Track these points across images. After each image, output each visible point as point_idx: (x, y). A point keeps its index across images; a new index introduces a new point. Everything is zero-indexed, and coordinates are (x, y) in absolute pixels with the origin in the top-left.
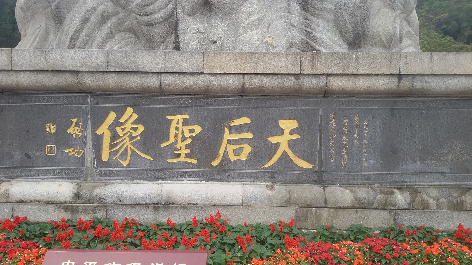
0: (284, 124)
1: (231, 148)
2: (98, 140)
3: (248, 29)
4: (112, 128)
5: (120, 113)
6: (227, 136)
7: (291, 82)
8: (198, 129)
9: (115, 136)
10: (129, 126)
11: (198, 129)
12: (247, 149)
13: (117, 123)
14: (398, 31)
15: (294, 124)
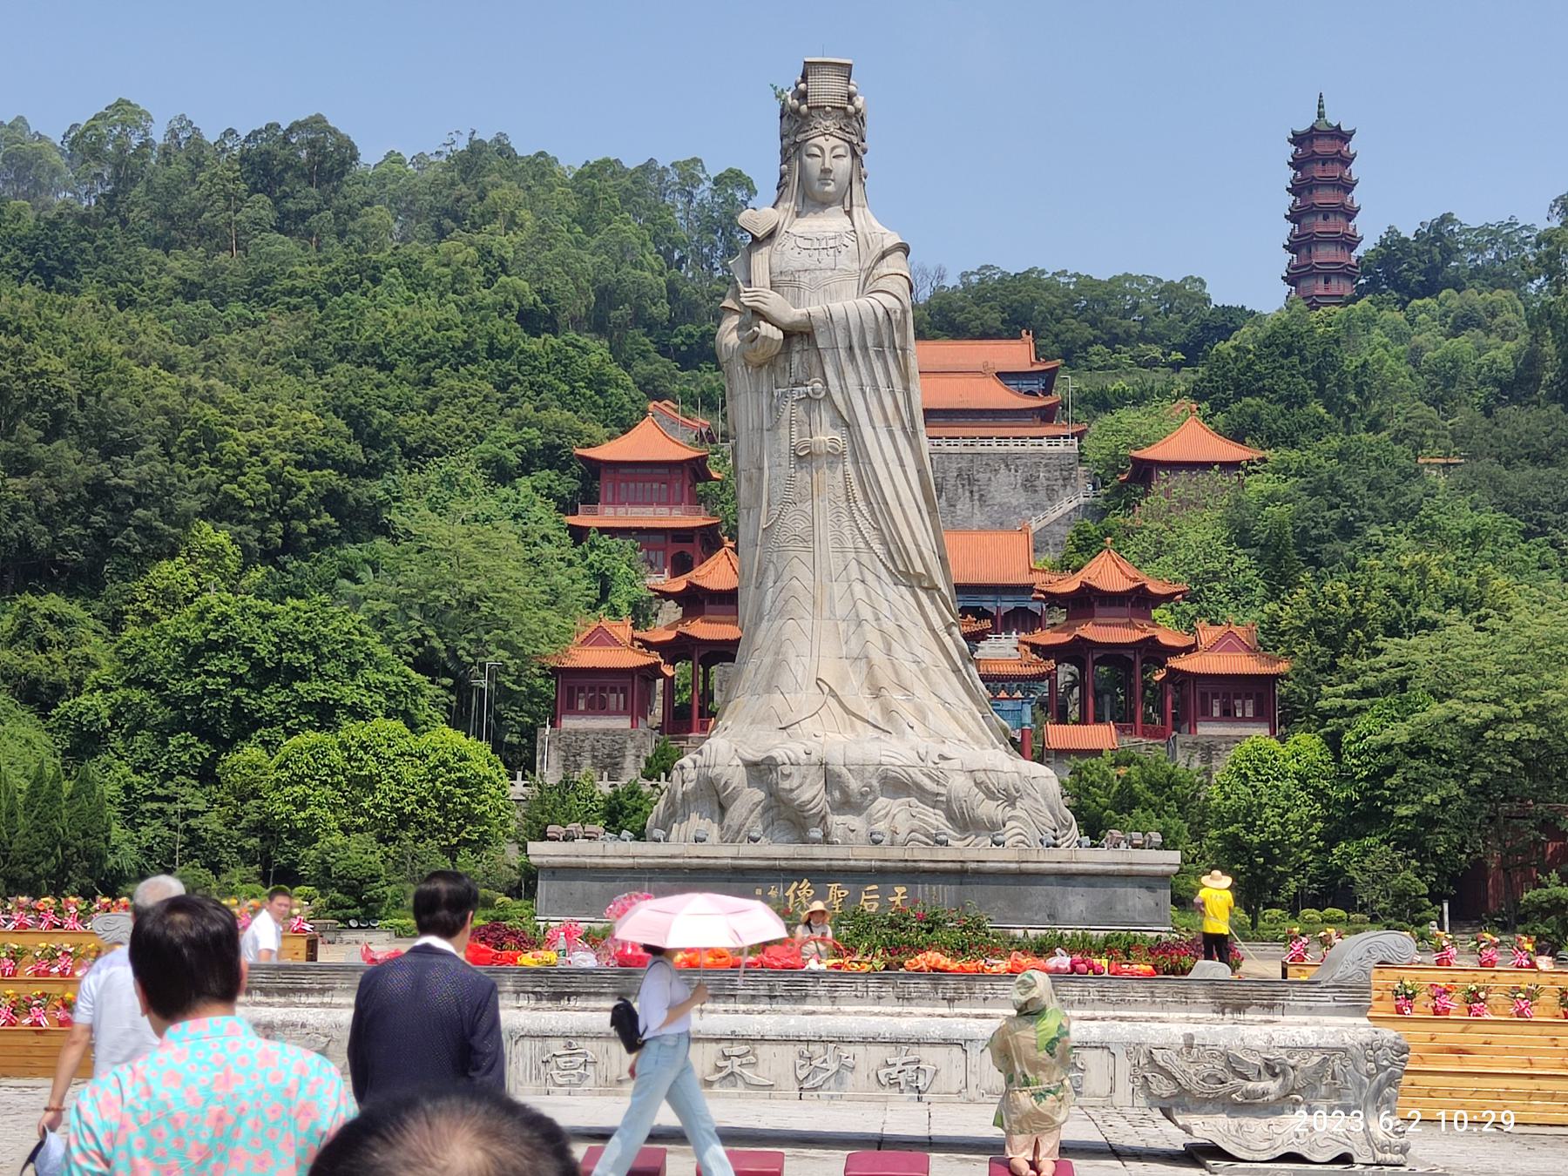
0: (897, 889)
1: (866, 904)
2: (787, 898)
3: (877, 821)
4: (794, 892)
5: (800, 882)
6: (864, 897)
7: (901, 864)
8: (846, 893)
9: (797, 897)
10: (805, 891)
11: (846, 893)
12: (876, 905)
13: (798, 889)
14: (1000, 817)
15: (904, 889)
